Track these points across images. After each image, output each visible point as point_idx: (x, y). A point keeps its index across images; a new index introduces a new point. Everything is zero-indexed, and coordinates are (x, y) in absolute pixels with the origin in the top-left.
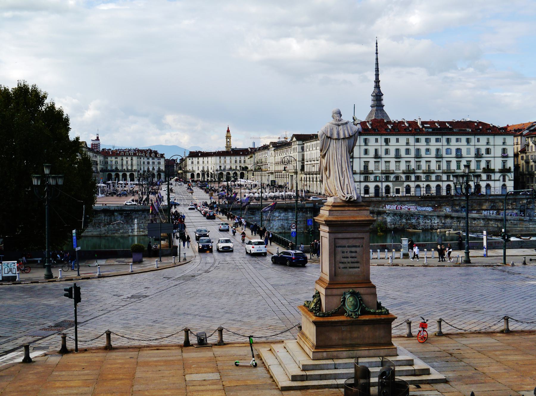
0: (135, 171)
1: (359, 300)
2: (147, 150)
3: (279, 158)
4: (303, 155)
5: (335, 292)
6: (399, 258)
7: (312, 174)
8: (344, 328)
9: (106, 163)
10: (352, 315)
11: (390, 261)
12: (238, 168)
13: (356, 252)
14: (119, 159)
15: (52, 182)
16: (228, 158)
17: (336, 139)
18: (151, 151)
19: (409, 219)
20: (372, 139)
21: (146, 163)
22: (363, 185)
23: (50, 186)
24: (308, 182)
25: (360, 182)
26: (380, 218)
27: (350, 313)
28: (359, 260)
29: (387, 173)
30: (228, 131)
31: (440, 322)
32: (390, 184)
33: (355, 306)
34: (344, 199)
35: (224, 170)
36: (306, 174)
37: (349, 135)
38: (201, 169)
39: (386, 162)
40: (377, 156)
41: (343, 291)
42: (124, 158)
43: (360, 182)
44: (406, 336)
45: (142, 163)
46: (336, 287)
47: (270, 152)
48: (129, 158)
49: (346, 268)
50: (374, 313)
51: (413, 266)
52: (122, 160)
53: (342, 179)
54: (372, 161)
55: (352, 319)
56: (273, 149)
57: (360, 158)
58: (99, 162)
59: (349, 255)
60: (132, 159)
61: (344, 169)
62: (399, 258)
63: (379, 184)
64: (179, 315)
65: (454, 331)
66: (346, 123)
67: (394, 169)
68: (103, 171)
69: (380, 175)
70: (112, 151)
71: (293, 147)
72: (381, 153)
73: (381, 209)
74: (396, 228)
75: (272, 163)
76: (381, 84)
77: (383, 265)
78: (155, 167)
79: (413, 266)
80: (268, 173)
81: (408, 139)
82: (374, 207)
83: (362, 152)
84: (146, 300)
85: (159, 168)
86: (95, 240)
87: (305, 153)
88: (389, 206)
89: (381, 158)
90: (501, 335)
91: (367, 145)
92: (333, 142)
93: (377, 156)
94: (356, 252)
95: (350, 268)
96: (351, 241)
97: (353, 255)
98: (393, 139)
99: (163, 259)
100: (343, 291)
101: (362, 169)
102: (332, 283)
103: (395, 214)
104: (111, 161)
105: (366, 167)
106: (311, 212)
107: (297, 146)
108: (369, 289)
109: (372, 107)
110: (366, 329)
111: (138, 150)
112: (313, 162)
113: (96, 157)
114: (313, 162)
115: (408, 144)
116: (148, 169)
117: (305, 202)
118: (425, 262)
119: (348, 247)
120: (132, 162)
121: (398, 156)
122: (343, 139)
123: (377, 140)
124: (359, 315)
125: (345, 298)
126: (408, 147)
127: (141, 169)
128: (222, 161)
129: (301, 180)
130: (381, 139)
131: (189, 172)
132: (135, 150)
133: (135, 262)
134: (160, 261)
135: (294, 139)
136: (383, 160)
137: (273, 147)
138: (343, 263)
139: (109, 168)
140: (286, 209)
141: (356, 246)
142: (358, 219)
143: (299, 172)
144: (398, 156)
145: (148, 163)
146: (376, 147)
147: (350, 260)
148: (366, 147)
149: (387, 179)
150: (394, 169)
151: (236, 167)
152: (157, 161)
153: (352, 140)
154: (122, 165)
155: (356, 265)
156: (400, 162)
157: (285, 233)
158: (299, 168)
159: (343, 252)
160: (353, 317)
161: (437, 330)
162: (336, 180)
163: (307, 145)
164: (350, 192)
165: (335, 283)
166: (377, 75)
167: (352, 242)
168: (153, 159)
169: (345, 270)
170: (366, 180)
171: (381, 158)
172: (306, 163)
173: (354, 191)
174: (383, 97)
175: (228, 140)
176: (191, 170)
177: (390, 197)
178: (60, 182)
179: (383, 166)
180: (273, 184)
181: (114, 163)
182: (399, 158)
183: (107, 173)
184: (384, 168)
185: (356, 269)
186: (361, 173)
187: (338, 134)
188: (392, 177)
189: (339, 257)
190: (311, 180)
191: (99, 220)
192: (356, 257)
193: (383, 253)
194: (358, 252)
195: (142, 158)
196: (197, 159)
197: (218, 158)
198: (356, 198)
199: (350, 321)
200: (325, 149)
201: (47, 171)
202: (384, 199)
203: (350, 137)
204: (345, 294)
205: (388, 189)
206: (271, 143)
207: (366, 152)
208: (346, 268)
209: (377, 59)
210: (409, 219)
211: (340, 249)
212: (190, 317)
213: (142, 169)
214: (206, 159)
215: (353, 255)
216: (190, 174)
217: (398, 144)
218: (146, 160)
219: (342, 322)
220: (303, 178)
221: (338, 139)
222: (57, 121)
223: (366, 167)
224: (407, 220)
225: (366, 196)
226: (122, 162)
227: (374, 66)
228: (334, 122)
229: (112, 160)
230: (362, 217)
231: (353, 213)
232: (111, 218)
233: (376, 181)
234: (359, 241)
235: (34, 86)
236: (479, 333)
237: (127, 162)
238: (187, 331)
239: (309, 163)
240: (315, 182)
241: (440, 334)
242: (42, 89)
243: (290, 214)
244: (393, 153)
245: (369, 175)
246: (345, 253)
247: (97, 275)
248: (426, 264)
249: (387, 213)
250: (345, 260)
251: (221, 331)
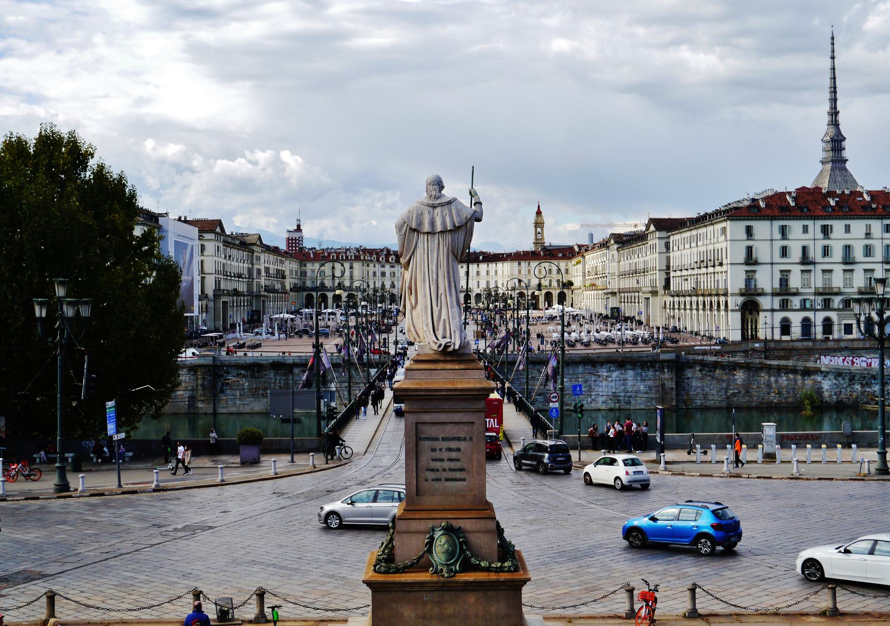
0: (358, 289)
1: (460, 543)
2: (382, 250)
3: (625, 265)
4: (668, 259)
5: (415, 525)
6: (756, 462)
7: (684, 296)
8: (426, 597)
9: (304, 274)
10: (442, 570)
11: (724, 468)
12: (555, 284)
13: (459, 450)
14: (327, 268)
15: (69, 312)
16: (534, 264)
17: (428, 233)
18: (388, 251)
19: (869, 385)
20: (795, 226)
22: (779, 316)
23: (64, 319)
24: (676, 311)
25: (773, 310)
26: (809, 382)
27: (439, 567)
28: (465, 466)
29: (827, 294)
30: (539, 213)
31: (693, 590)
32: (833, 315)
33: (450, 554)
34: (435, 348)
35: (527, 287)
36: (672, 296)
37: (454, 225)
38: (483, 285)
39: (824, 271)
40: (805, 260)
41: (430, 524)
42: (338, 266)
43: (773, 310)
44: (624, 615)
45: (371, 274)
46: (417, 516)
47: (611, 253)
48: (347, 265)
49: (440, 480)
50: (488, 569)
51: (770, 478)
52: (333, 268)
53: (436, 309)
54: (796, 270)
55: (442, 579)
56: (616, 246)
57: (772, 264)
58: (287, 273)
59: (445, 455)
60: (351, 268)
61: (441, 291)
62: (756, 462)
63: (810, 315)
64: (241, 564)
65: (718, 608)
66: (449, 203)
67: (841, 285)
68: (296, 289)
69: (812, 298)
71: (650, 243)
72: (816, 253)
73: (810, 364)
74: (842, 401)
75: (613, 274)
76: (841, 118)
77: (711, 476)
79: (770, 478)
80: (607, 294)
81: (869, 227)
82: (798, 360)
83: (777, 252)
84: (202, 536)
86: (258, 420)
87: (671, 255)
88: (828, 358)
89: (815, 263)
90: (818, 619)
91: (786, 239)
92: (423, 239)
93: (805, 260)
94: (459, 450)
95: (447, 480)
96: (448, 428)
97: (454, 455)
98: (838, 226)
99: (296, 457)
100: (430, 524)
101: (777, 285)
102: (411, 508)
103: (839, 374)
105: (784, 282)
106: (670, 369)
107: (657, 241)
108: (482, 521)
109: (823, 163)
110: (471, 598)
111: (365, 251)
112: (685, 273)
113: (282, 262)
114: (685, 273)
115: (868, 235)
116: (383, 285)
117: (659, 350)
118: (795, 470)
119: (444, 439)
120: (351, 273)
121: (848, 260)
122: (441, 232)
123: (805, 229)
124: (456, 572)
125: (432, 538)
126: (868, 242)
127: (368, 286)
128: (524, 271)
129: (665, 307)
130: (815, 226)
132: (358, 250)
133: (244, 464)
134: (292, 461)
135: (652, 228)
136: (819, 268)
137: (616, 242)
138: (433, 470)
140: (621, 363)
141: (458, 439)
142: (460, 386)
143: (661, 292)
144: (848, 260)
145: (383, 274)
146: (805, 243)
147: (446, 465)
148: (784, 243)
149: (827, 306)
150: (841, 285)
151: (551, 281)
153: (461, 235)
155: (458, 475)
156: (852, 271)
157: (620, 410)
158: (660, 284)
159: (434, 450)
160: (443, 576)
161: (687, 606)
162: (426, 313)
163: (676, 238)
164: (448, 335)
165: (416, 508)
166: (834, 100)
167: (450, 431)
168: (392, 267)
169: (436, 485)
170: (784, 306)
171: (815, 263)
172: (672, 274)
173: (458, 334)
174: (845, 144)
175: (539, 230)
177: (834, 340)
178: (85, 312)
179: (817, 280)
180: (616, 314)
182: (852, 264)
183: (305, 294)
184: (820, 284)
185: (460, 483)
186: (774, 294)
187: (432, 223)
188: (837, 301)
189: (426, 458)
190: (682, 307)
191: (265, 382)
192: (458, 460)
193: (723, 452)
194: (462, 449)
195: (371, 265)
196: (475, 266)
197: (516, 264)
198: (457, 347)
199: (436, 583)
200: (407, 252)
201: (60, 292)
202: (818, 345)
203: (456, 229)
204: (433, 530)
205: (828, 325)
206: (613, 236)
207: (784, 252)
208: (440, 480)
209: (833, 69)
210: (867, 384)
211: (427, 444)
212: (256, 568)
213: (372, 286)
214: (492, 266)
215: (454, 455)
217: (848, 236)
218: (378, 269)
219: (421, 584)
220: (668, 304)
221: (432, 233)
222: (112, 197)
223: (784, 282)
224: (863, 386)
225: (785, 338)
227: (828, 83)
228: (426, 201)
229: (312, 268)
230: (469, 382)
231: (451, 375)
232: (287, 379)
233: (803, 308)
234: (465, 428)
235: (72, 134)
236: (776, 614)
238: (197, 595)
239: (679, 273)
240: (688, 311)
241: (694, 614)
242: (87, 137)
243: (631, 373)
244: (838, 254)
245: (791, 298)
246: (438, 452)
247: (153, 486)
248: (797, 475)
249: (822, 372)
250: (438, 465)
251: (261, 595)
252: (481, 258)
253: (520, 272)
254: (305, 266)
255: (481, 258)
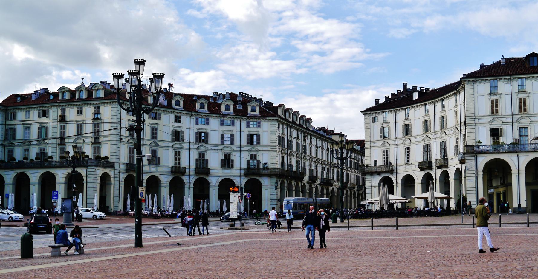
21: (189, 136)
35: (516, 147)
38: (417, 156)
42: (71, 113)
48: (89, 111)
52: (63, 118)
70: (73, 93)
78: (235, 157)
85: (253, 157)
104: (27, 128)
131: (372, 174)
139: (18, 155)
145: (202, 138)
152: (246, 131)
154: (62, 139)
176: (380, 163)
181: (34, 134)
214: (434, 109)
216: (377, 179)
226: (63, 129)
237: (79, 127)
252: (415, 96)
253: (495, 107)
254: (14, 117)
255: (415, 96)
